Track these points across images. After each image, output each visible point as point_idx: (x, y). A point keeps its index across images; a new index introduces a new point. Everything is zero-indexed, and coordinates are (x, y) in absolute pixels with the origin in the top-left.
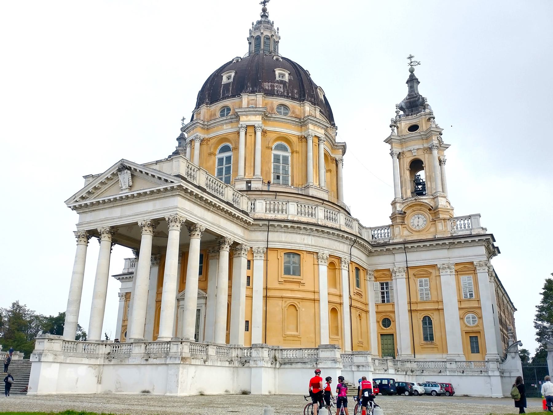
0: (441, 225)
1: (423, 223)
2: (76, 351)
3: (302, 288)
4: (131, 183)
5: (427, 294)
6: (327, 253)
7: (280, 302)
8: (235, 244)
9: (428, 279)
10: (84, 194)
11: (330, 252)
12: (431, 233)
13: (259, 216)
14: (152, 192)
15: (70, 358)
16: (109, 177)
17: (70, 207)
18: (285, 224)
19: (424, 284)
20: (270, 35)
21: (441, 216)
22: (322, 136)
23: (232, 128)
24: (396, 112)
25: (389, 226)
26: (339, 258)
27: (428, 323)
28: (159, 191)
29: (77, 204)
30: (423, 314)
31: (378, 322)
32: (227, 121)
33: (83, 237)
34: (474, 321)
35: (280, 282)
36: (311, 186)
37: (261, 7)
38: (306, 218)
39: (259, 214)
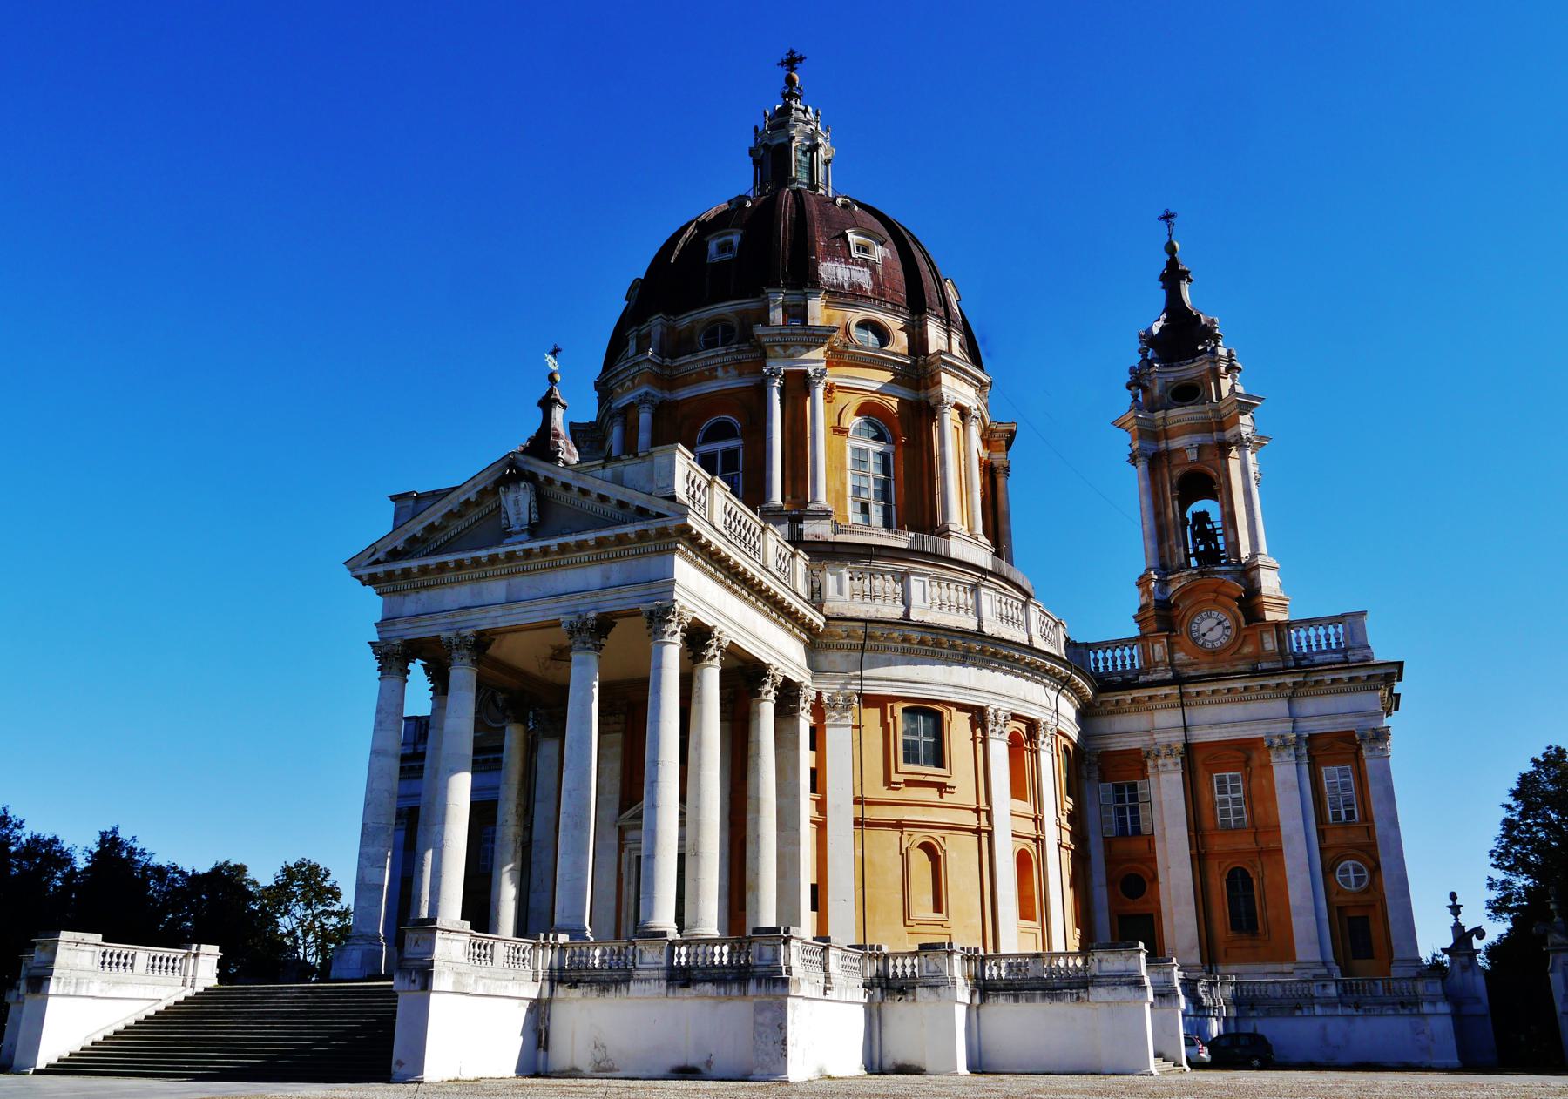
0: (1270, 640)
1: (1224, 632)
2: (492, 961)
3: (947, 798)
4: (537, 517)
5: (1239, 813)
6: (1006, 706)
7: (894, 835)
9: (1240, 774)
10: (400, 544)
11: (1012, 707)
12: (1245, 657)
13: (835, 611)
14: (600, 543)
15: (484, 981)
16: (473, 499)
17: (359, 577)
18: (906, 633)
19: (1229, 788)
21: (1270, 616)
22: (972, 404)
23: (740, 375)
24: (1139, 352)
25: (1137, 639)
26: (1033, 726)
27: (1240, 885)
28: (621, 540)
29: (380, 569)
30: (1229, 861)
31: (1110, 883)
32: (727, 358)
33: (396, 659)
34: (1359, 880)
35: (894, 783)
36: (954, 534)
37: (783, 72)
38: (953, 618)
39: (840, 604)
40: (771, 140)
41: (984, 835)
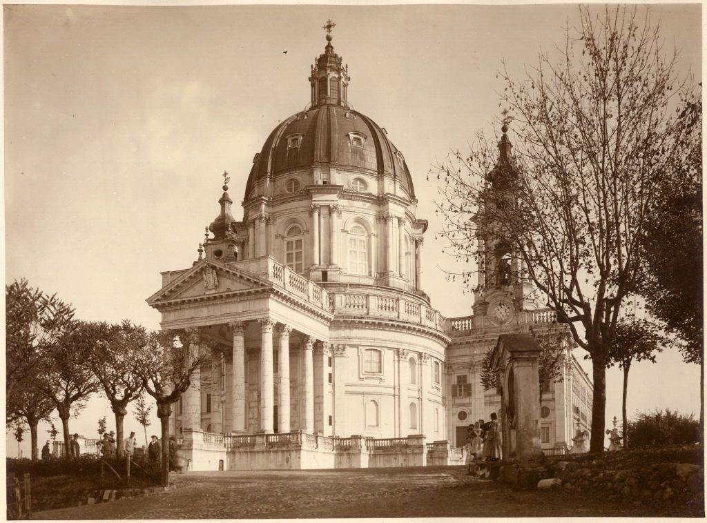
7: (361, 397)
8: (318, 341)
10: (166, 293)
17: (152, 306)
20: (337, 76)
29: (159, 303)
40: (319, 75)
41: (397, 397)
